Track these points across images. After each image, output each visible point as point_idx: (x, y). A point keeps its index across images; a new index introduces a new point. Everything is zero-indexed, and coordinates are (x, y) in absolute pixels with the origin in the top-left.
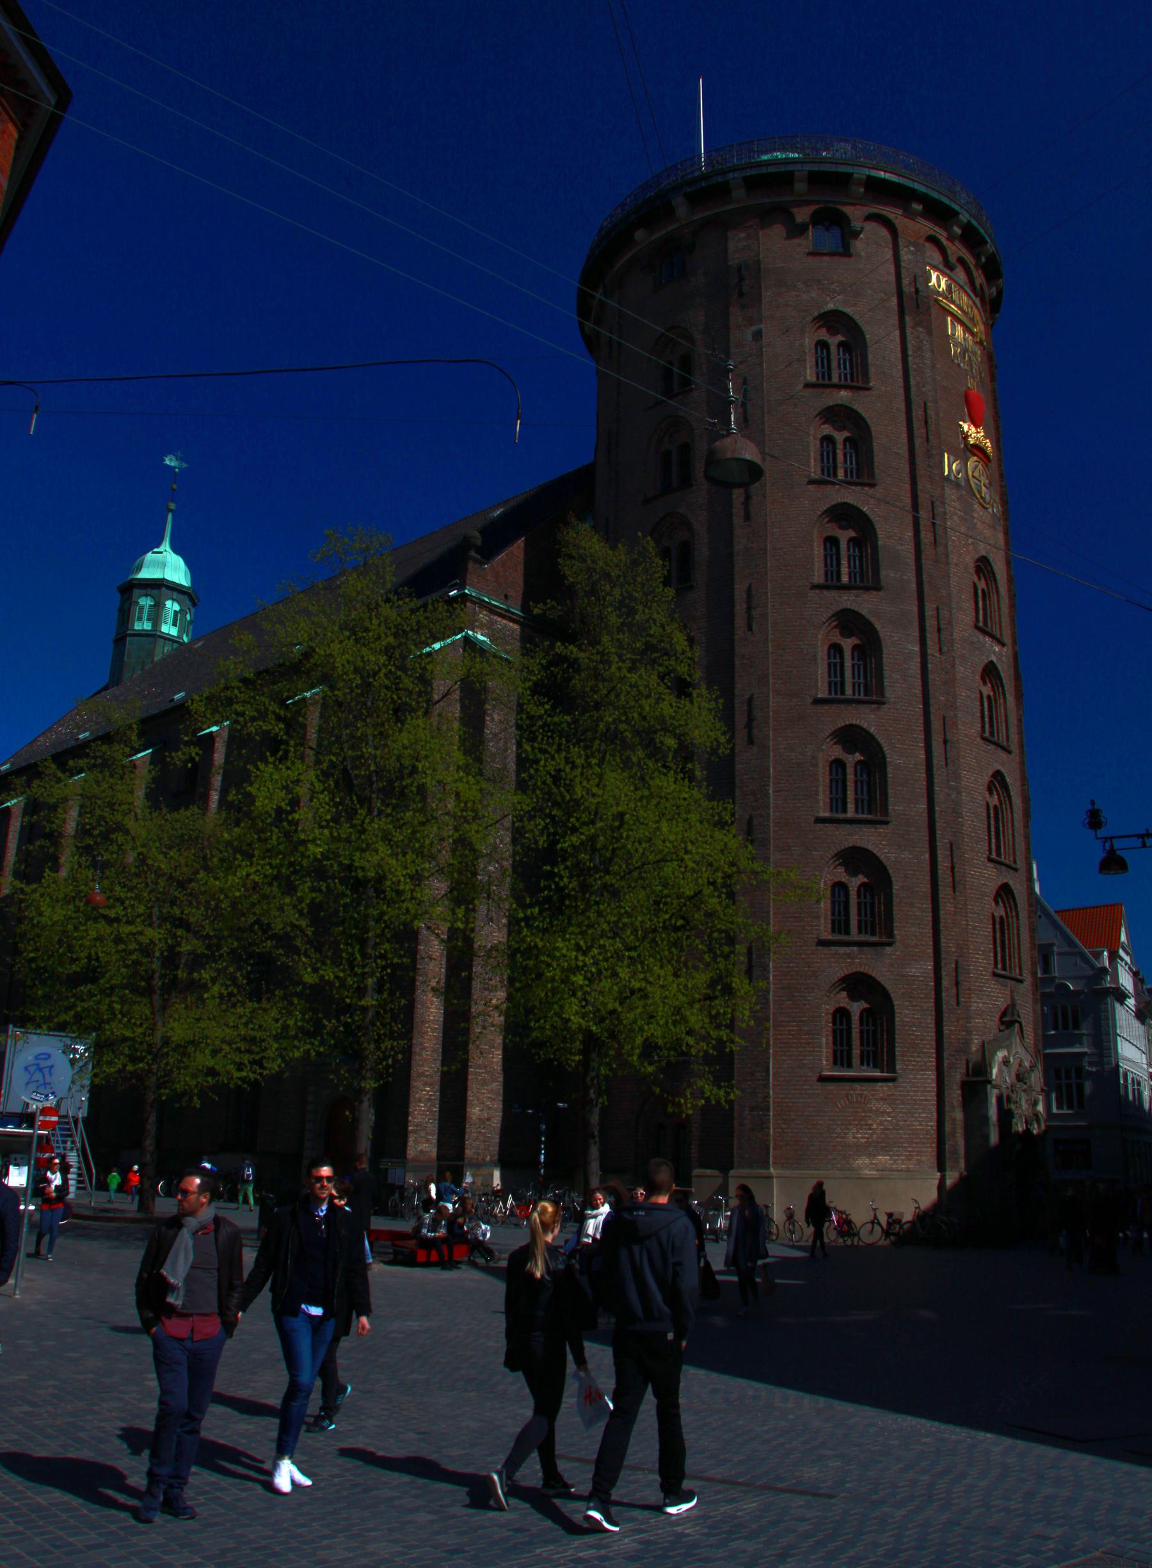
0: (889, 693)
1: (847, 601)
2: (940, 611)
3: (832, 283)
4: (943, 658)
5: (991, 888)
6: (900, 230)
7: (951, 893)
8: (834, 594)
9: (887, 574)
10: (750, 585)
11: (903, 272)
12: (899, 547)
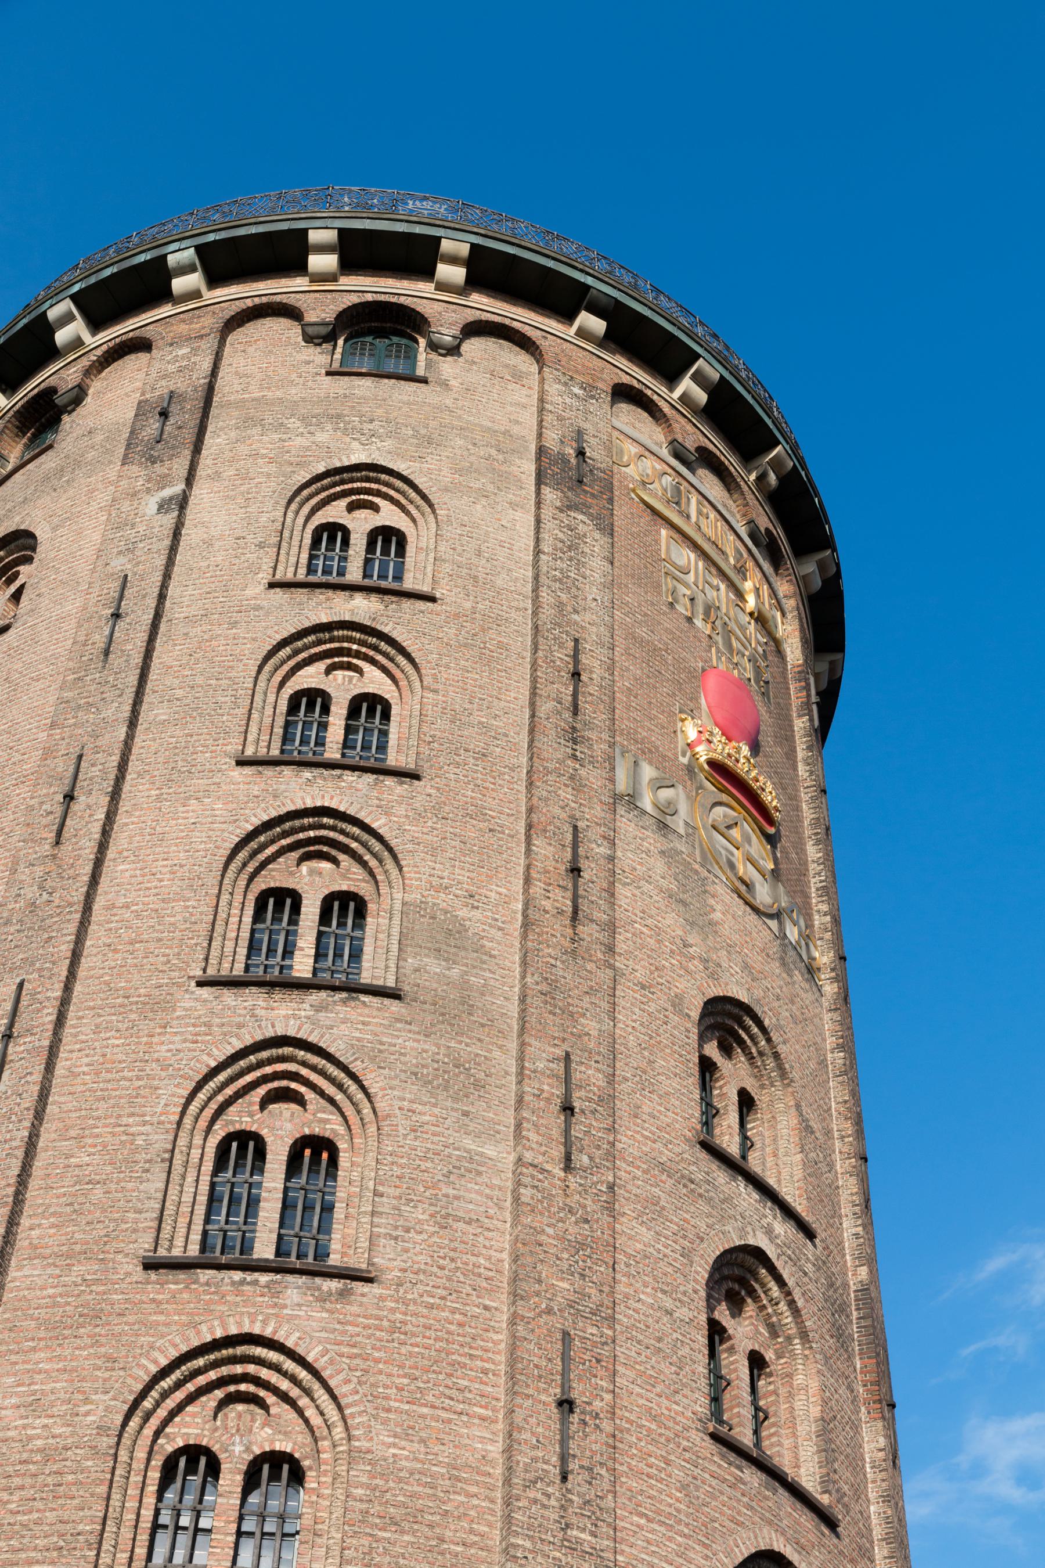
3: (371, 421)
6: (548, 357)
8: (254, 999)
10: (21, 985)
11: (549, 418)
12: (463, 913)
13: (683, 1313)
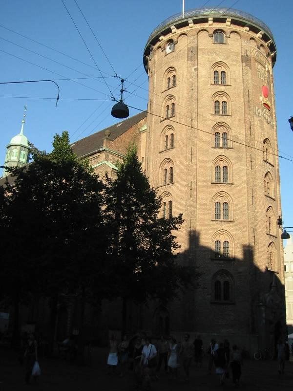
1: (221, 152)
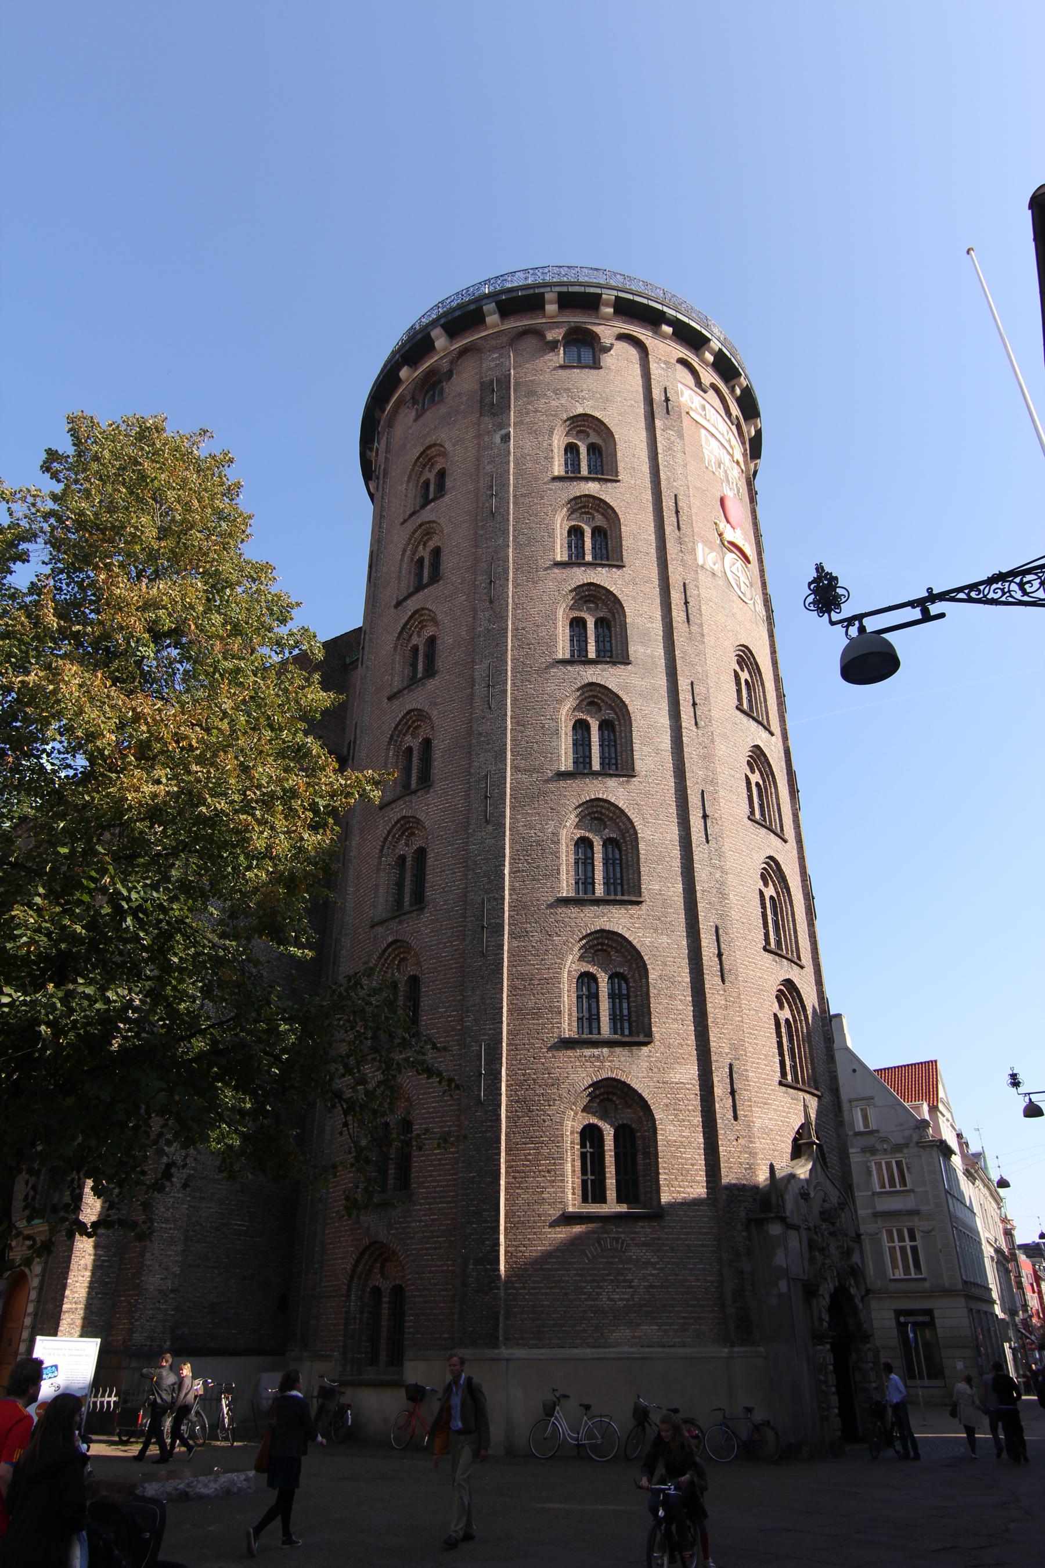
0: (639, 765)
2: (695, 686)
3: (582, 391)
4: (700, 732)
5: (773, 985)
7: (720, 983)
9: (635, 649)
13: (738, 776)
